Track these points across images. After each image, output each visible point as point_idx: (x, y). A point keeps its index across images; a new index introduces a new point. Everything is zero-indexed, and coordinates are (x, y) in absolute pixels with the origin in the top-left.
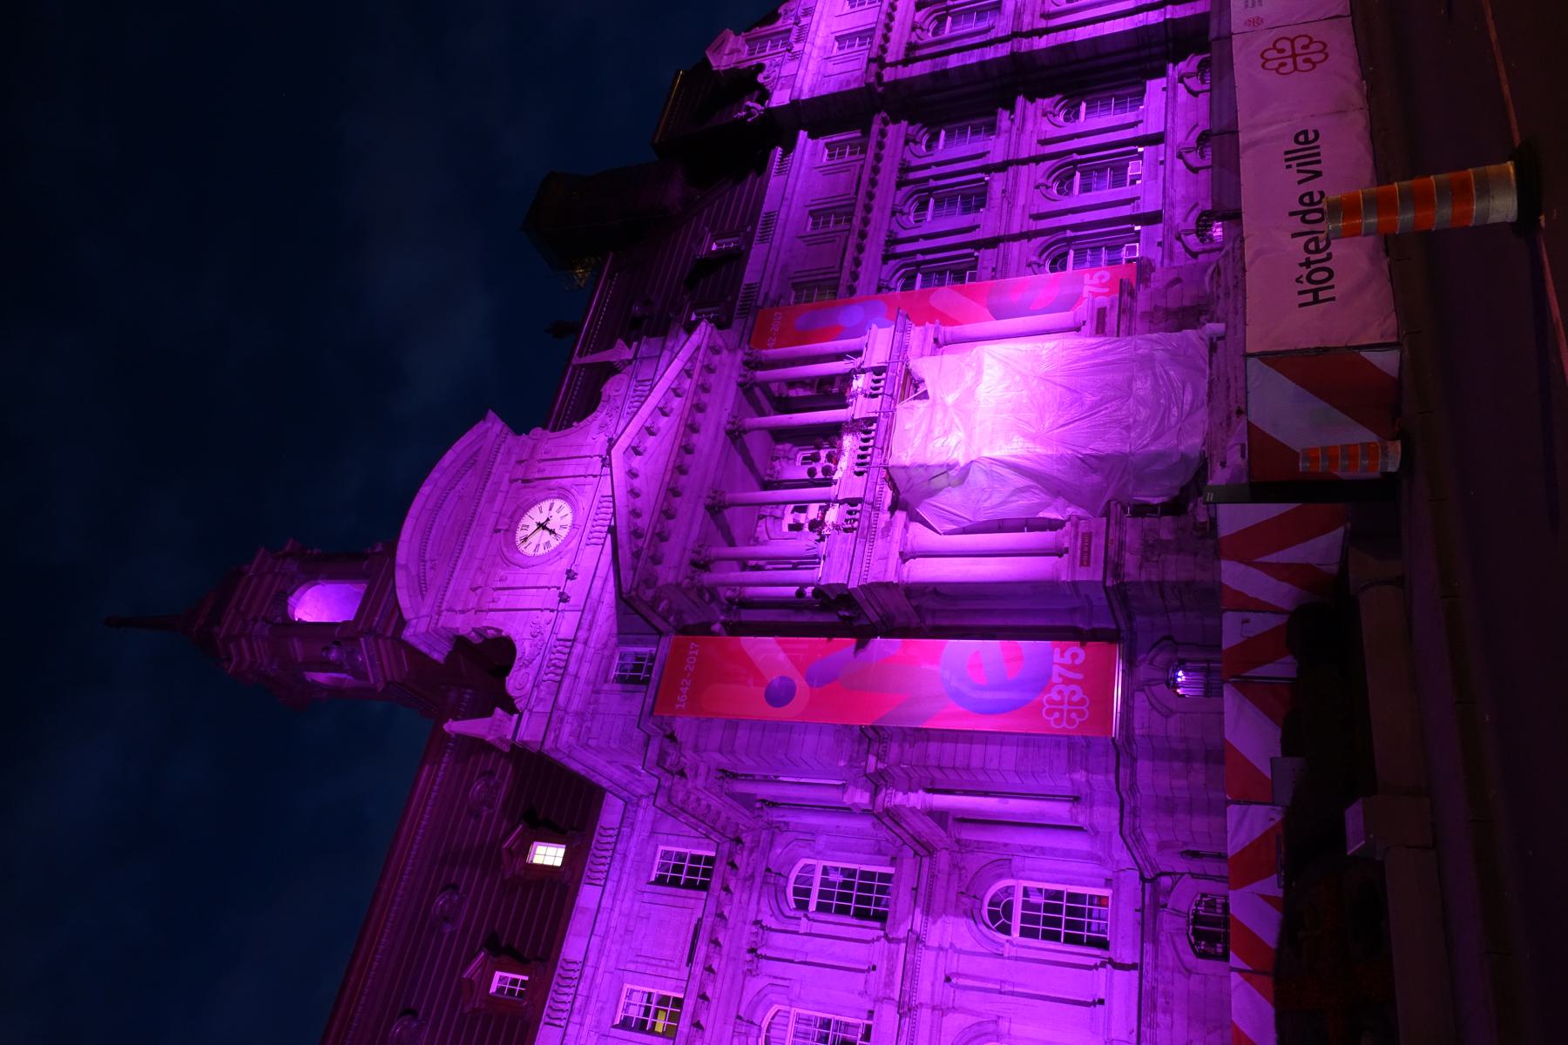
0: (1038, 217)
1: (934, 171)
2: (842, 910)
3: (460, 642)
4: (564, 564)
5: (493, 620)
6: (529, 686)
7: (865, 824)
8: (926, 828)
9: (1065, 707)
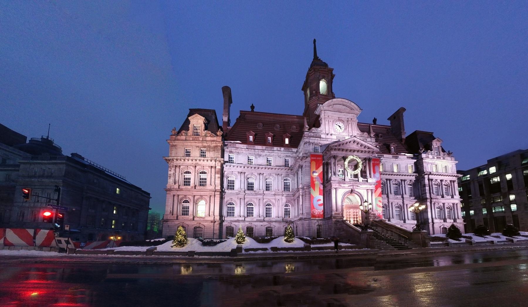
0: (392, 203)
1: (403, 186)
4: (333, 133)
5: (323, 122)
7: (296, 187)
8: (297, 195)
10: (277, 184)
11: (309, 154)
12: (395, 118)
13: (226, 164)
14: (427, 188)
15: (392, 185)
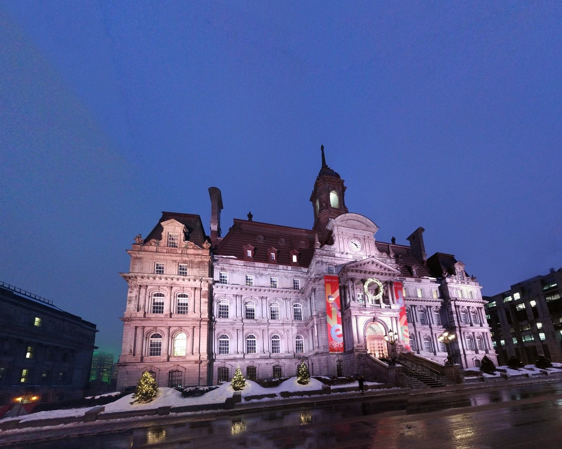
0: (419, 333)
2: (295, 313)
3: (331, 232)
4: (349, 252)
5: (336, 239)
7: (310, 315)
8: (311, 324)
12: (414, 238)
13: (217, 284)
14: (455, 315)
15: (417, 312)
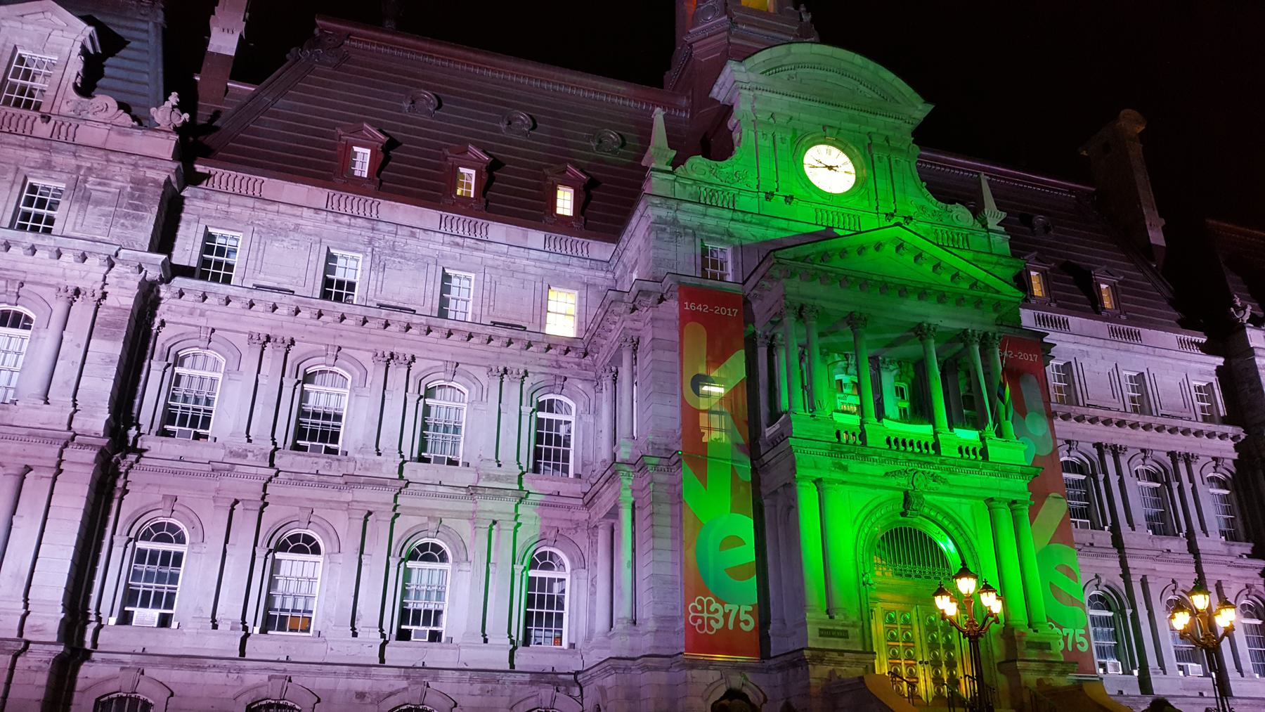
2: (539, 438)
3: (728, 110)
4: (797, 191)
6: (695, 176)
7: (605, 454)
8: (605, 503)
9: (705, 615)
10: (484, 421)
11: (668, 282)
13: (179, 282)
